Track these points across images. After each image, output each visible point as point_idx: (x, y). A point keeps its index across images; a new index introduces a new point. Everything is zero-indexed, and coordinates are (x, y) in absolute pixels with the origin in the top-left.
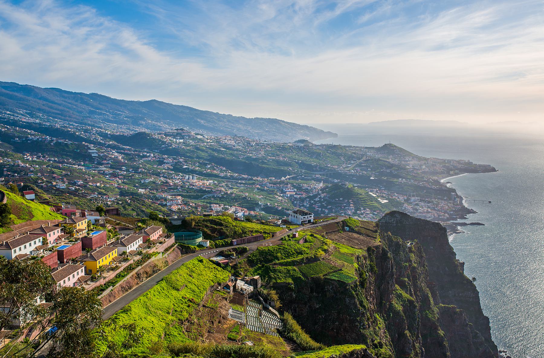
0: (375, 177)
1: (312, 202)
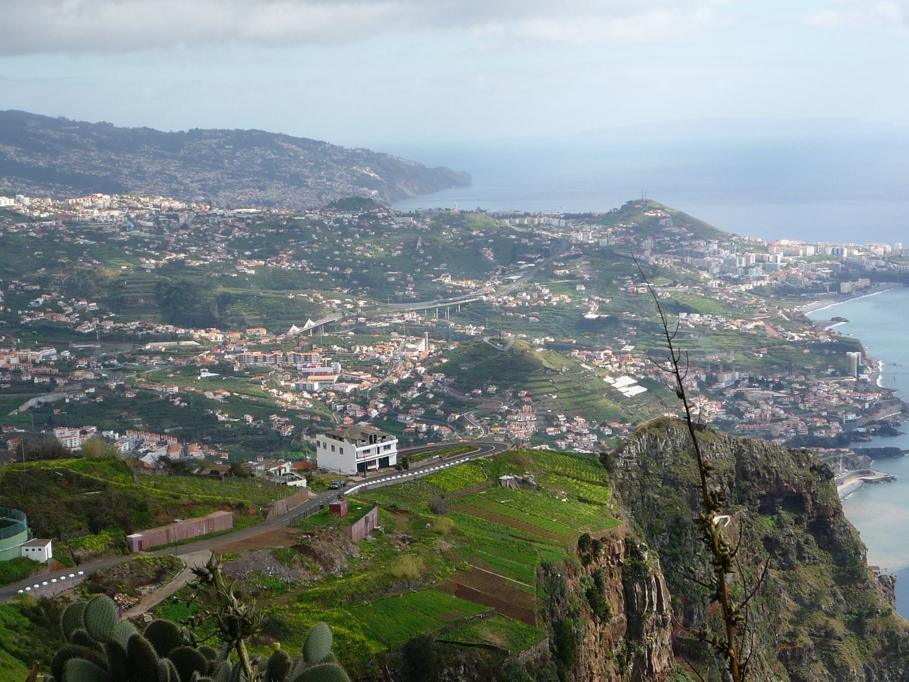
0: (602, 309)
1: (396, 402)
